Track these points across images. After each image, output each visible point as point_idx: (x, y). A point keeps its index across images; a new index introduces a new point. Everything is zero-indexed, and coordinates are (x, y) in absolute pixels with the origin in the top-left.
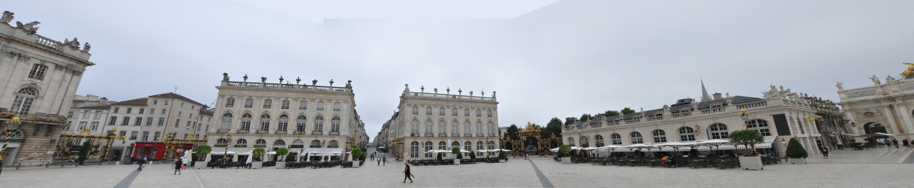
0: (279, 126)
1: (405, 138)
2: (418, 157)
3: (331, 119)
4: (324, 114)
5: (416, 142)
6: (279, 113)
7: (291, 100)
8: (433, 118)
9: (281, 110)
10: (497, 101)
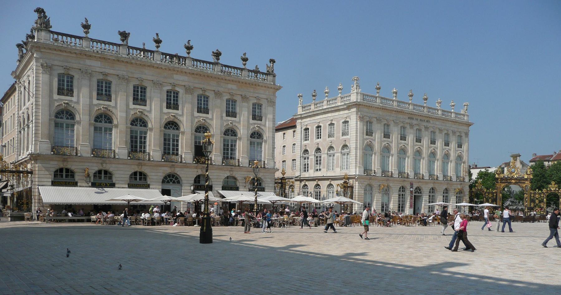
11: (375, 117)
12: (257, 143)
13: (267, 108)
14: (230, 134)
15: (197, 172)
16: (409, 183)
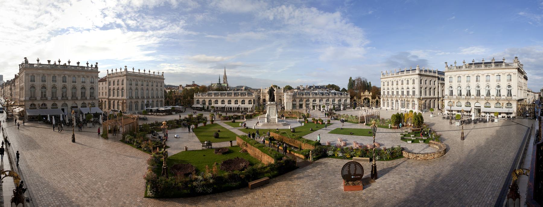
0: (81, 94)
6: (61, 85)
7: (67, 76)
9: (62, 83)
10: (164, 78)
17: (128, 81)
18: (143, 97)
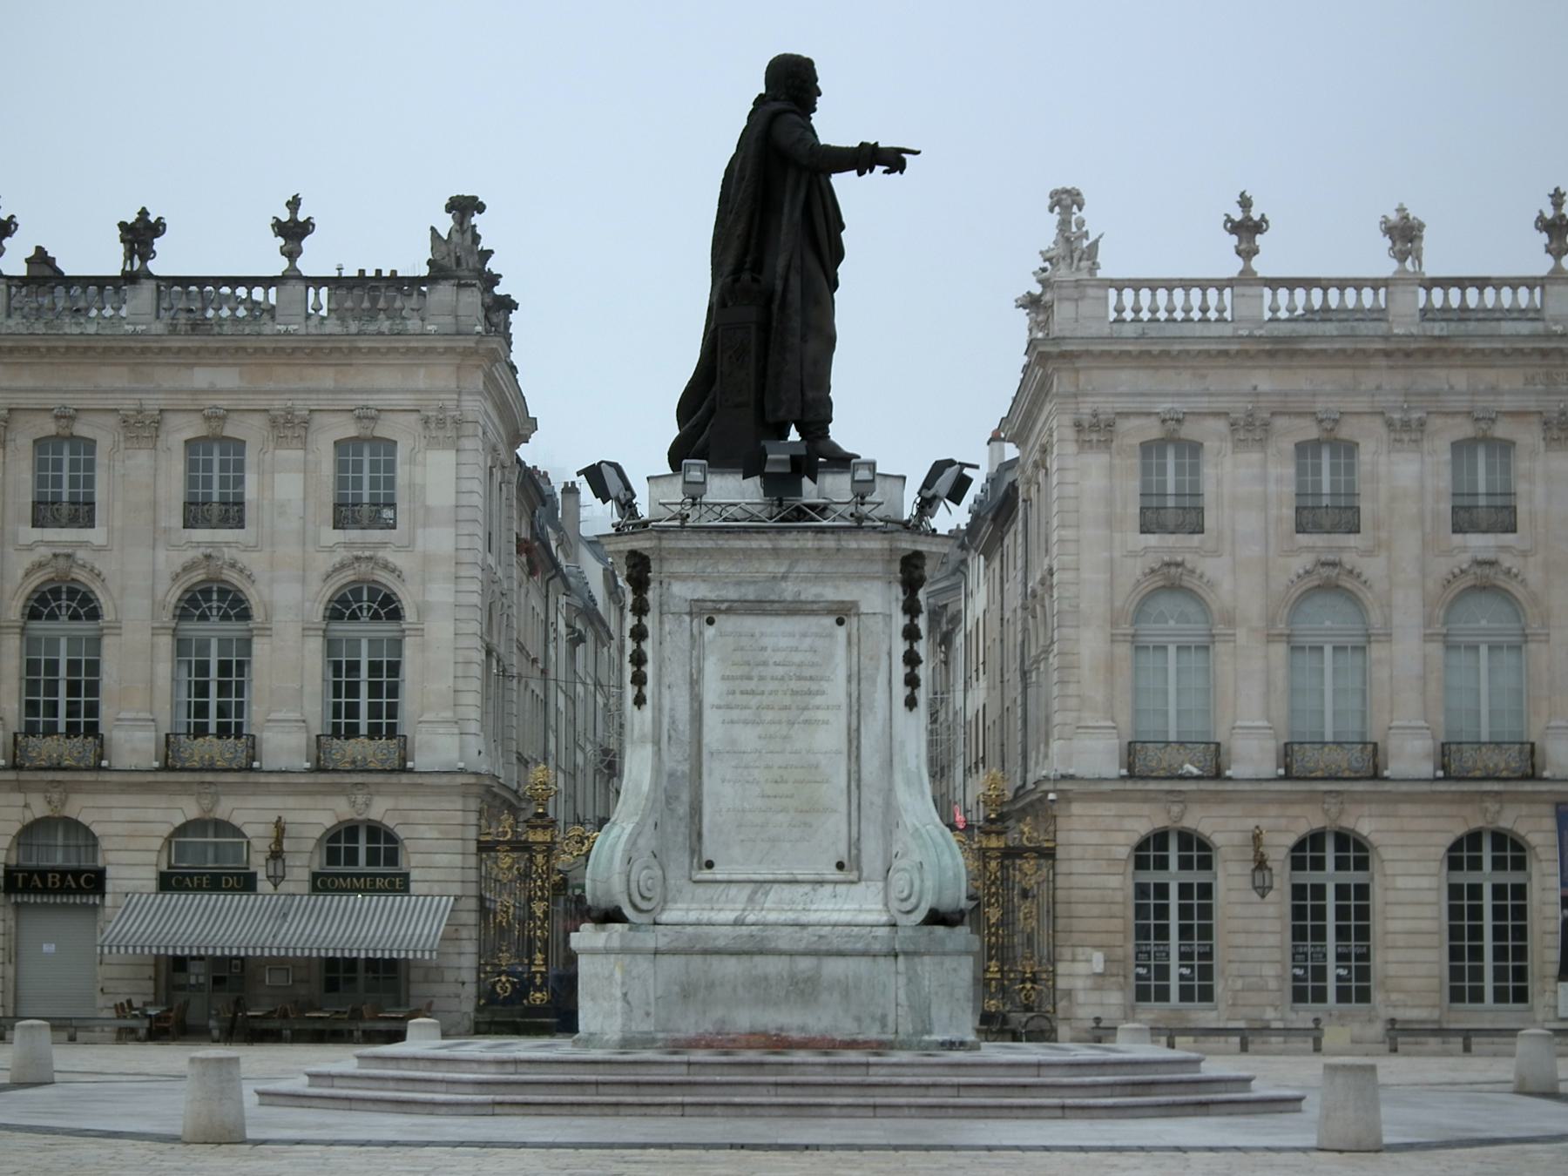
1: (1065, 798)
2: (1207, 995)
3: (317, 612)
4: (254, 562)
5: (1188, 840)
8: (1373, 568)
11: (1216, 414)
12: (370, 641)
13: (420, 457)
14: (215, 612)
15: (26, 806)
16: (1549, 810)
17: (1096, 462)
18: (1507, 760)
